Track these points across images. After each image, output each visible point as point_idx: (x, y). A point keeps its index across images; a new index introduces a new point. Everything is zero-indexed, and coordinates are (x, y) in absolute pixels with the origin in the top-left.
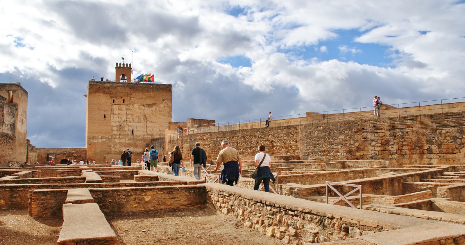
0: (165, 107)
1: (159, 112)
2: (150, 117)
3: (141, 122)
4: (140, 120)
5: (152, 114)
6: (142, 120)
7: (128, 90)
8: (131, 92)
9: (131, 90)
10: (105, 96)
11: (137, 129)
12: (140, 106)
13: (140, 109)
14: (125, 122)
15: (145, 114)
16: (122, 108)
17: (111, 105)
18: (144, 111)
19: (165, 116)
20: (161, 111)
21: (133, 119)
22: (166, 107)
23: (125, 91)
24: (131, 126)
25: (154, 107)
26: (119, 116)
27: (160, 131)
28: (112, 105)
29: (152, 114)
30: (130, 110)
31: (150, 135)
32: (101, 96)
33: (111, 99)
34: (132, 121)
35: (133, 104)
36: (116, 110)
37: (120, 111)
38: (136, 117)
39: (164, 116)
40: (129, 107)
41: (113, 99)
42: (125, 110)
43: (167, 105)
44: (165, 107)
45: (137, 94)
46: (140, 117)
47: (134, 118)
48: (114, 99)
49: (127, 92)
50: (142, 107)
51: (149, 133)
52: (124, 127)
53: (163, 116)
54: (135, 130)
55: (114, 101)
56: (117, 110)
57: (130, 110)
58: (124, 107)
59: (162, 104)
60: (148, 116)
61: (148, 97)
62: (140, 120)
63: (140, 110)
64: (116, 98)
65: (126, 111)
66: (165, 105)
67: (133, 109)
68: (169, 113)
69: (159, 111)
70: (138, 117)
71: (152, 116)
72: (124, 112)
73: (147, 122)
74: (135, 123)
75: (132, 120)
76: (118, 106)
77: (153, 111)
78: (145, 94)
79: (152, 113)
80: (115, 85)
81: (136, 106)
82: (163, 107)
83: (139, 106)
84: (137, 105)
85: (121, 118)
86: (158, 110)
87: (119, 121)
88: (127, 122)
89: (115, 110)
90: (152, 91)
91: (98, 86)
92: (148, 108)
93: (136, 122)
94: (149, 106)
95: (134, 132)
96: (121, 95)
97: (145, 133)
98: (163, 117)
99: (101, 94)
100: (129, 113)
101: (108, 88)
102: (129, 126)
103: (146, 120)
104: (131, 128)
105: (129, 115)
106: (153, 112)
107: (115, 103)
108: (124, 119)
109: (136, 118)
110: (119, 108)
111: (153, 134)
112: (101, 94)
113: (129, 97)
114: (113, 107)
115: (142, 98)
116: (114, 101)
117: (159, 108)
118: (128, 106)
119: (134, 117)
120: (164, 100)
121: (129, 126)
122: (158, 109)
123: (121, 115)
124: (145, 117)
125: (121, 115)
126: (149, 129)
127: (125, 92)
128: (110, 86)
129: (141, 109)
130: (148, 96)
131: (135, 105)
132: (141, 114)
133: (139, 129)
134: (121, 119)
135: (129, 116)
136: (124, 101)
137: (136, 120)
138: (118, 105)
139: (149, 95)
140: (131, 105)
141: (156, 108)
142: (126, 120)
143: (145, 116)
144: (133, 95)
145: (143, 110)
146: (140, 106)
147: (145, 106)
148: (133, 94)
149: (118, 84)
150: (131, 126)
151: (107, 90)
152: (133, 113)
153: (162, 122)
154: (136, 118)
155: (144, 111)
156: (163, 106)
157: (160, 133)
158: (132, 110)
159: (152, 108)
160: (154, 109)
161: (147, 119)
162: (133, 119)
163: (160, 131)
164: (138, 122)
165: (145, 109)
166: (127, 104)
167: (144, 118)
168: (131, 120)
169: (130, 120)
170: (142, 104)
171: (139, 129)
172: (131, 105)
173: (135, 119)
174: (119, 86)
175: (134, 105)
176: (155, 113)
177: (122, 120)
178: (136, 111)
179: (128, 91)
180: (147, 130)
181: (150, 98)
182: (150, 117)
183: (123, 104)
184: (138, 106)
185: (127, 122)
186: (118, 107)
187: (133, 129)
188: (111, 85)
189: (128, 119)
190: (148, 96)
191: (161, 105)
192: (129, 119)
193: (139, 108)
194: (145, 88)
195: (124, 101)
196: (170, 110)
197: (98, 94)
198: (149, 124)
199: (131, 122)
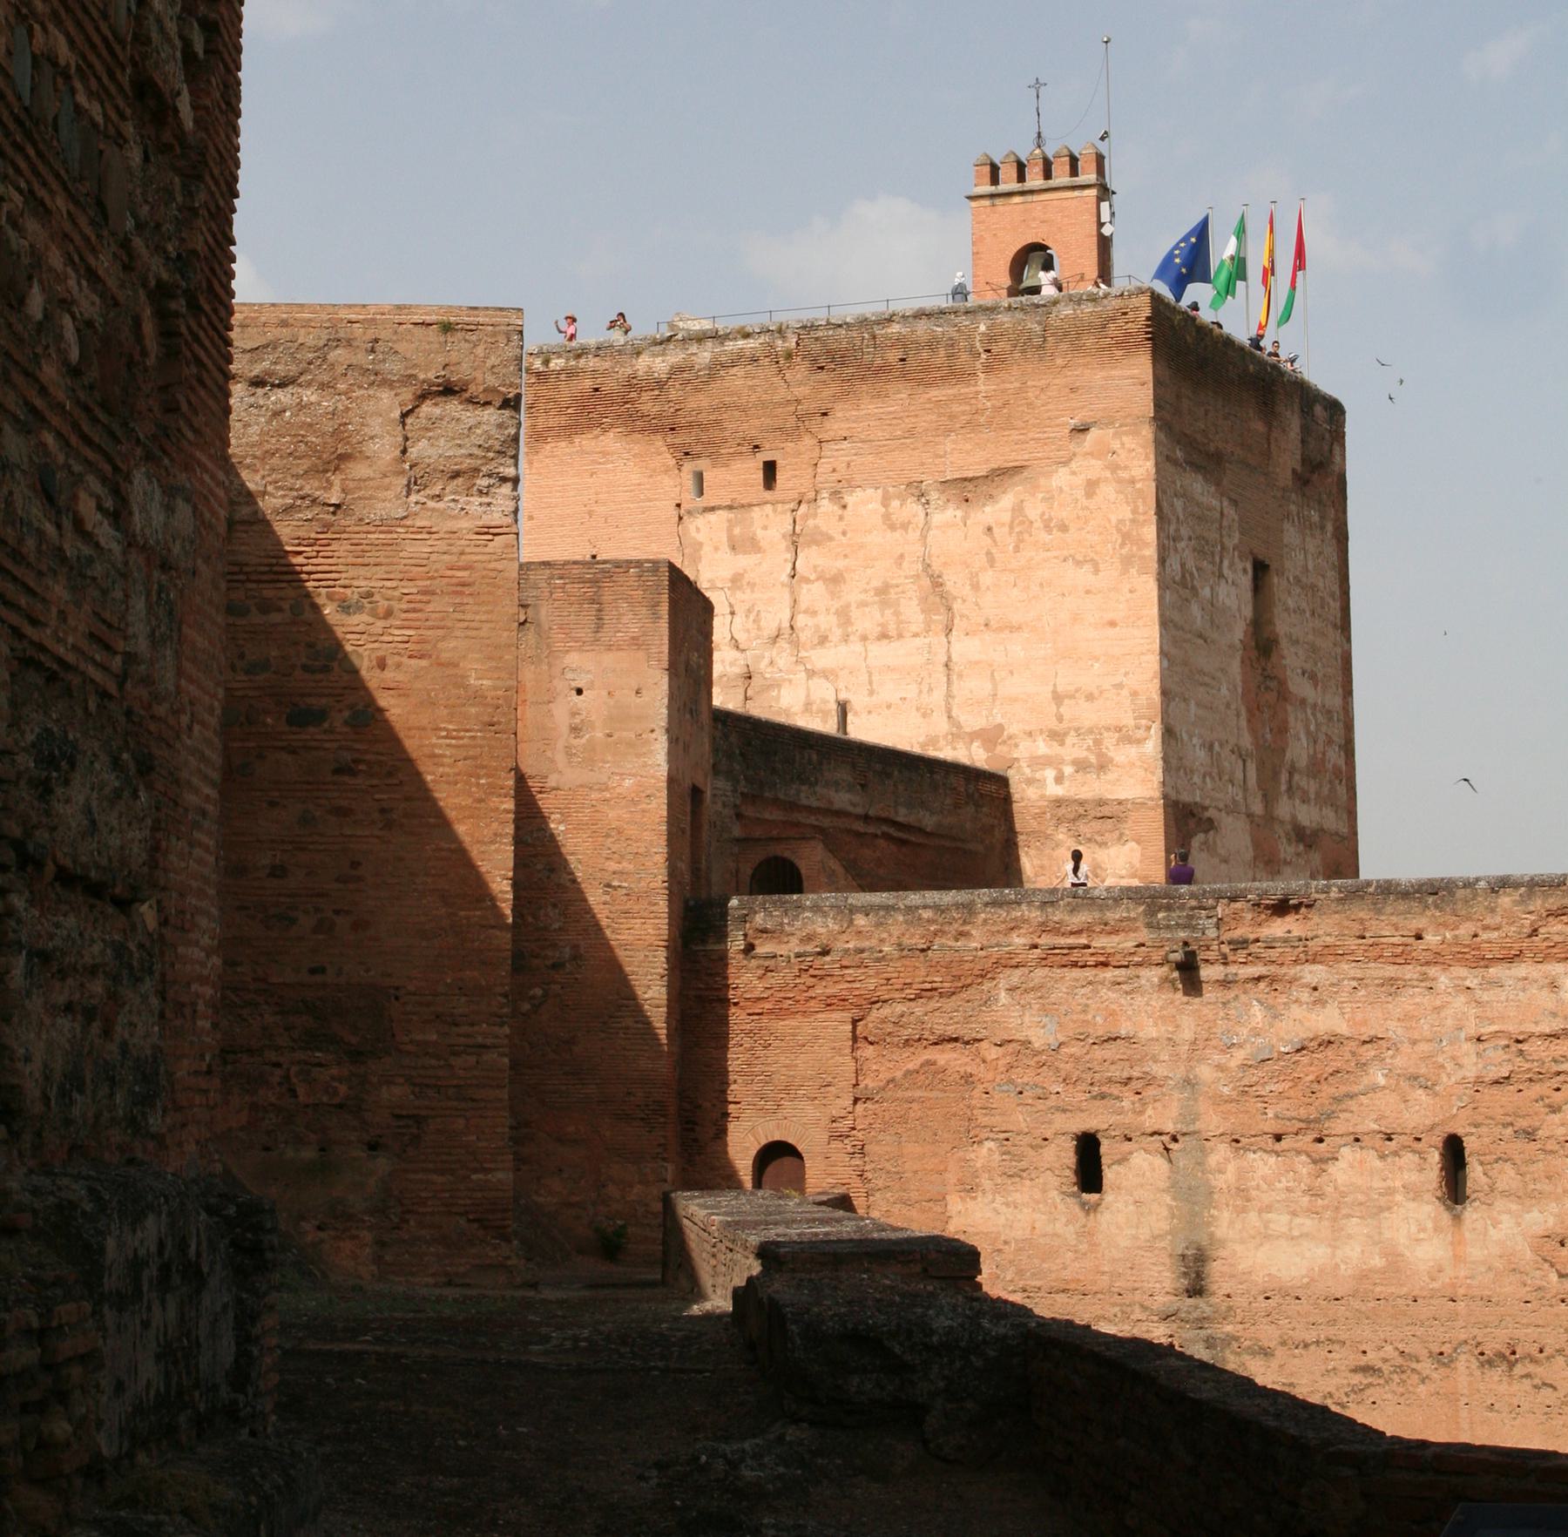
0: (1091, 487)
1: (1044, 537)
2: (976, 587)
3: (900, 636)
4: (897, 614)
5: (991, 561)
6: (912, 612)
7: (801, 383)
8: (827, 393)
9: (823, 375)
10: (637, 449)
11: (871, 693)
12: (896, 503)
13: (892, 527)
14: (782, 643)
15: (936, 567)
16: (760, 533)
17: (680, 518)
18: (924, 537)
19: (1097, 571)
20: (1064, 528)
21: (844, 616)
22: (1107, 491)
23: (782, 393)
24: (826, 674)
25: (1007, 501)
26: (739, 595)
27: (1058, 698)
28: (689, 512)
29: (991, 561)
30: (819, 539)
31: (974, 736)
32: (604, 454)
33: (679, 467)
34: (837, 634)
35: (836, 495)
36: (716, 549)
37: (744, 561)
38: (863, 596)
39: (1087, 567)
40: (811, 522)
41: (689, 467)
42: (783, 544)
43: (1114, 468)
44: (1091, 487)
45: (870, 407)
46: (892, 595)
47: (848, 606)
48: (702, 464)
49: (798, 401)
50: (914, 508)
51: (972, 721)
52: (777, 685)
53: (1078, 563)
54: (857, 701)
55: (699, 477)
56: (725, 554)
57: (819, 539)
58: (770, 523)
59: (1073, 465)
60: (955, 581)
61: (952, 417)
62: (897, 614)
63: (898, 534)
64: (714, 457)
65: (789, 556)
66: (1095, 468)
67: (844, 533)
68: (1126, 537)
69: (1048, 528)
70: (883, 591)
71: (987, 578)
72: (776, 561)
73: (949, 630)
74: (857, 647)
75: (833, 619)
76: (732, 516)
77: (995, 530)
78: (934, 393)
79: (988, 553)
80: (704, 355)
81: (865, 503)
82: (1080, 494)
83: (885, 501)
84: (870, 491)
85: (749, 611)
86: (1038, 524)
87: (741, 637)
88: (796, 644)
89: (706, 550)
90: (988, 369)
91: (588, 384)
92: (959, 513)
93: (864, 638)
94: (967, 489)
95: (850, 717)
96: (752, 427)
97: (941, 725)
98: (1084, 576)
99: (611, 441)
100: (815, 567)
101: (661, 385)
102: (811, 674)
103: (940, 618)
104: (825, 694)
105: (807, 581)
106: (994, 541)
107: (709, 498)
108: (777, 616)
109: (863, 604)
110: (737, 531)
111: (1000, 728)
112: (611, 434)
113: (808, 441)
114: (692, 528)
115: (910, 433)
116: (699, 477)
117: (1049, 499)
118: (803, 507)
119: (852, 593)
120: (1082, 430)
121: (811, 674)
122: (1034, 510)
123: (752, 585)
124: (936, 588)
125: (752, 585)
126: (973, 686)
127: (777, 398)
128: (676, 370)
129: (905, 526)
130: (956, 408)
131: (859, 493)
132: (905, 565)
133: (889, 691)
134: (750, 625)
135: (813, 593)
136: (770, 469)
137: (867, 621)
138: (730, 508)
139: (964, 400)
140: (825, 504)
141: (1018, 509)
142: (786, 624)
143: (937, 583)
144: (839, 415)
145: (914, 535)
146: (896, 503)
147: (934, 495)
148: (838, 406)
149: (730, 346)
150: (826, 674)
151: (648, 404)
152: (841, 564)
153: (1076, 618)
154: (863, 604)
155: (924, 537)
156: (1080, 480)
157: (1060, 719)
158: (831, 539)
159: (988, 509)
160: (1006, 517)
161: (950, 609)
162: (844, 616)
163: (1058, 698)
164: (884, 636)
165: (937, 518)
166: (794, 495)
167: (923, 600)
168: (827, 621)
169: (817, 627)
170: (909, 485)
171: (889, 691)
172: (825, 504)
173: (855, 613)
174: (737, 360)
175: (849, 499)
176: (1017, 549)
177: (759, 629)
178: (862, 546)
179: (799, 391)
180: (949, 695)
181: (971, 425)
182: (976, 587)
183: (768, 495)
184: (875, 506)
185: (796, 644)
186: (730, 530)
187: (843, 696)
188: (675, 357)
189: (801, 620)
190: (956, 408)
191: (1063, 471)
192: (814, 613)
193: (887, 517)
194: (932, 345)
195: (770, 469)
196: (1135, 511)
197: (585, 441)
198: (965, 648)
199: (823, 640)
